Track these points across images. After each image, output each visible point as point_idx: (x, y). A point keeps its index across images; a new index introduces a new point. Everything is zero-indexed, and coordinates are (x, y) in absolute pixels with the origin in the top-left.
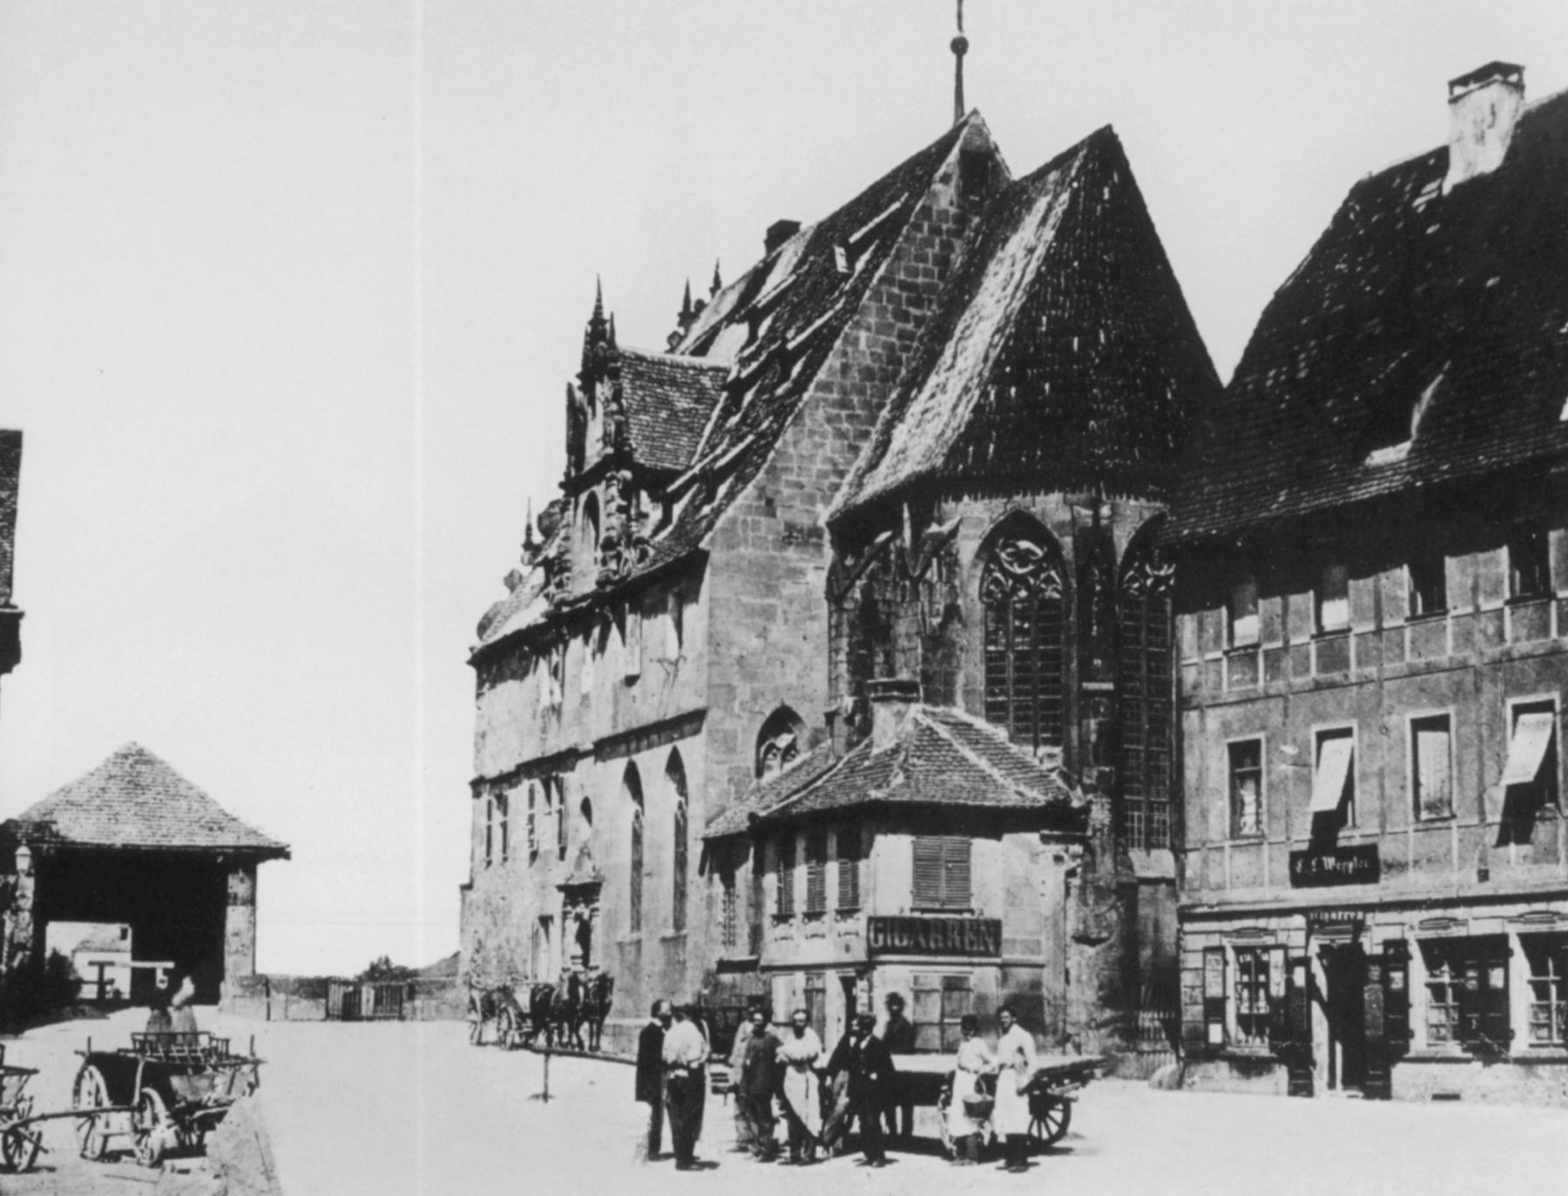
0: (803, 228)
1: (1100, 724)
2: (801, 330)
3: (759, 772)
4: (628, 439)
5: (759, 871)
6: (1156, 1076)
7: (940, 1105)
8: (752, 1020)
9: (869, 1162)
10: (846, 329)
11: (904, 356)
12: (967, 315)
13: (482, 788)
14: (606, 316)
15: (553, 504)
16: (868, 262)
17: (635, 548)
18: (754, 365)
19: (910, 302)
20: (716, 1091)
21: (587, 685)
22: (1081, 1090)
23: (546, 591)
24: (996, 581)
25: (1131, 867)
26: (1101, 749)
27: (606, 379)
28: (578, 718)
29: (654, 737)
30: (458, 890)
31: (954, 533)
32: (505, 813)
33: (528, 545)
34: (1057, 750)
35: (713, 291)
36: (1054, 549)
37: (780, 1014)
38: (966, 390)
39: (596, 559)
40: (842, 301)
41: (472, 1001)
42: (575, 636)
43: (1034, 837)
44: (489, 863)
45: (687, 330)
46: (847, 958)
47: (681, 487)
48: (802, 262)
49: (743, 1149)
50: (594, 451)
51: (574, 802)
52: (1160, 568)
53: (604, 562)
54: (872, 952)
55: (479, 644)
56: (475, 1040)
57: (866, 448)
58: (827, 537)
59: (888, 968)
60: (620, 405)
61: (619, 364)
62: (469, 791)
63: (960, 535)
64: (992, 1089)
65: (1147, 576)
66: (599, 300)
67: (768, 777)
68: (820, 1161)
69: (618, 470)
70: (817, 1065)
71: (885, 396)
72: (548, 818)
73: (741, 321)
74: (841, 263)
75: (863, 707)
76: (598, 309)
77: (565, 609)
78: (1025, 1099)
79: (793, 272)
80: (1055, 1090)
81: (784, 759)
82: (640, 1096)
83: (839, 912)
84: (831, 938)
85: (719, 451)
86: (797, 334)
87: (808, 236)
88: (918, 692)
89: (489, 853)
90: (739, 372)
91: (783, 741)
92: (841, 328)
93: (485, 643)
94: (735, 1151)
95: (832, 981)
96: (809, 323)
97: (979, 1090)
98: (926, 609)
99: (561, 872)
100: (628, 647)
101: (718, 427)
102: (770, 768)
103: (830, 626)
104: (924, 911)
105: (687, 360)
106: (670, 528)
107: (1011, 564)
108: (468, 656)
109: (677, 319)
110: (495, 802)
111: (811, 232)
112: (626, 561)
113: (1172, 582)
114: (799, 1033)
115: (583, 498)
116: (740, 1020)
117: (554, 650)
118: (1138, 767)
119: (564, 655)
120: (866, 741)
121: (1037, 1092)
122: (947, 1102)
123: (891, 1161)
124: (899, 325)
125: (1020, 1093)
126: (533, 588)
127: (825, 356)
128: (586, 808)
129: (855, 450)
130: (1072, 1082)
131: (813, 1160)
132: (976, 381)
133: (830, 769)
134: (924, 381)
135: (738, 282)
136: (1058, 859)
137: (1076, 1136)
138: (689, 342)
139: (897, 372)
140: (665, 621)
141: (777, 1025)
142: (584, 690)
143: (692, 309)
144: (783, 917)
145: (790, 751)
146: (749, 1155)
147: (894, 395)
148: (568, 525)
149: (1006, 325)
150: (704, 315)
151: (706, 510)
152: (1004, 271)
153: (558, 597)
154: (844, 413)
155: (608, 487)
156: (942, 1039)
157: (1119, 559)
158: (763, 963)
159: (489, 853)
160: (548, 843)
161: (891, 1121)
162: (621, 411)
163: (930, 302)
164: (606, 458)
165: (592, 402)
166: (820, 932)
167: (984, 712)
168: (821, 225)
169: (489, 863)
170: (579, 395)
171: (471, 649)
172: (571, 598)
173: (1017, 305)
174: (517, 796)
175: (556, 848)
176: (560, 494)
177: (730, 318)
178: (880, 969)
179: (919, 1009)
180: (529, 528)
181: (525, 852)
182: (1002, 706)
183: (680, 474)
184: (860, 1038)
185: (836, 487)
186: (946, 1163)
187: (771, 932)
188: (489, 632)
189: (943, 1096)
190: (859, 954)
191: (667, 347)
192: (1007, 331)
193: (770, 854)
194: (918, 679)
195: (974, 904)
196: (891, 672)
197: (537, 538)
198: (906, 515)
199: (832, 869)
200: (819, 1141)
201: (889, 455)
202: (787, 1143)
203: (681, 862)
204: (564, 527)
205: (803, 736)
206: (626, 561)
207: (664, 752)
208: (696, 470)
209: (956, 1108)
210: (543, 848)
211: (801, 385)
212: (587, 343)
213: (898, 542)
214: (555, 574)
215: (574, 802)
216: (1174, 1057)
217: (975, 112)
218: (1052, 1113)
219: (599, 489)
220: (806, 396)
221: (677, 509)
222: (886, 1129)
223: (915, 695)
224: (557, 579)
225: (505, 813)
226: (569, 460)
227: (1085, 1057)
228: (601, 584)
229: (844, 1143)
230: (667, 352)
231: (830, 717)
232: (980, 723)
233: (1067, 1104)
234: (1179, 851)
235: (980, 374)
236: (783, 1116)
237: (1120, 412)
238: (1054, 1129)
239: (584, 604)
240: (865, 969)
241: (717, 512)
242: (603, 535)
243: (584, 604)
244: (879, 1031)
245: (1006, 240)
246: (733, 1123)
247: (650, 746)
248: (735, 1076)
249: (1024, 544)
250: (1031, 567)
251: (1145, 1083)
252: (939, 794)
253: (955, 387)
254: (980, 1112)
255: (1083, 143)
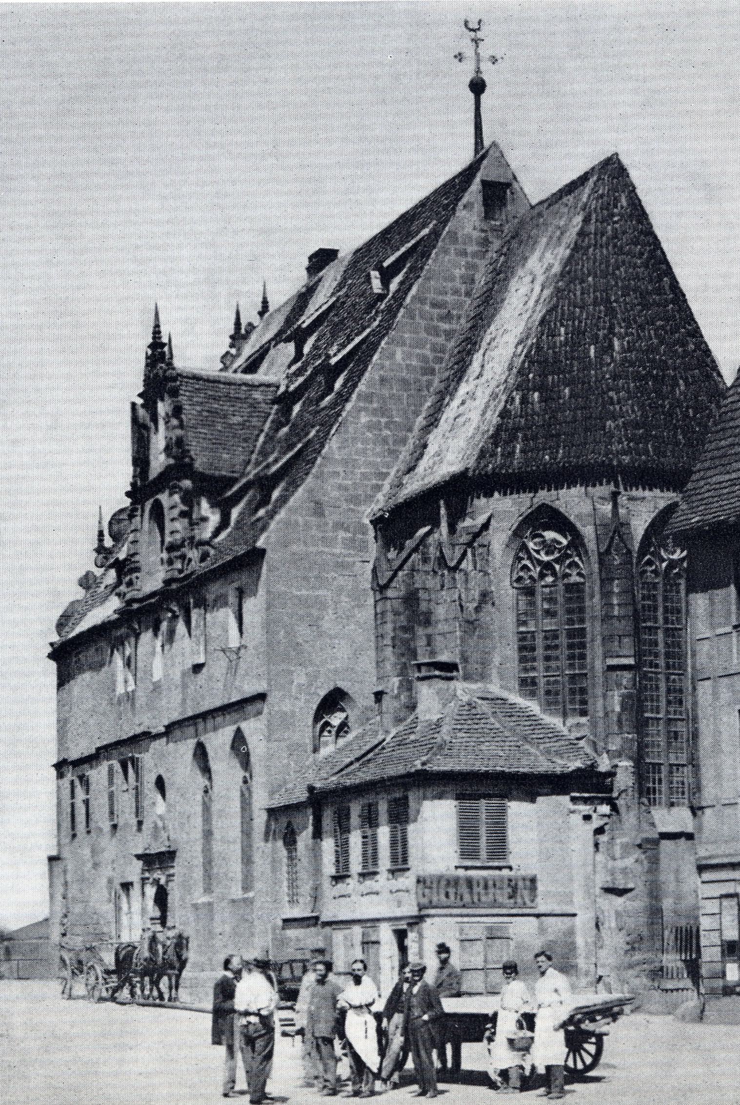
0: (340, 255)
1: (623, 696)
2: (343, 346)
3: (316, 750)
4: (189, 451)
5: (318, 834)
6: (679, 1011)
7: (485, 1041)
8: (315, 970)
9: (423, 1093)
10: (383, 343)
11: (437, 367)
12: (492, 328)
13: (64, 769)
14: (165, 340)
15: (122, 511)
16: (402, 283)
17: (197, 548)
18: (301, 380)
19: (442, 318)
20: (285, 1034)
21: (158, 674)
22: (612, 1024)
23: (117, 590)
24: (525, 567)
25: (653, 825)
26: (624, 717)
27: (166, 396)
28: (150, 706)
29: (219, 720)
30: (46, 862)
31: (486, 526)
32: (87, 792)
33: (100, 549)
34: (583, 720)
35: (261, 314)
36: (577, 542)
37: (340, 964)
38: (494, 396)
39: (162, 560)
40: (379, 319)
41: (63, 960)
42: (147, 629)
43: (565, 800)
44: (74, 836)
45: (239, 350)
46: (398, 913)
47: (237, 492)
48: (340, 287)
49: (310, 1085)
50: (159, 461)
51: (149, 779)
52: (673, 553)
53: (170, 562)
54: (421, 908)
55: (55, 638)
56: (66, 996)
57: (405, 453)
58: (371, 533)
59: (436, 920)
60: (181, 421)
61: (178, 383)
62: (53, 772)
63: (490, 531)
64: (531, 1027)
65: (663, 560)
66: (157, 326)
67: (324, 752)
68: (380, 1093)
69: (179, 480)
70: (375, 1008)
71: (421, 405)
72: (126, 794)
73: (288, 340)
74: (376, 285)
75: (407, 686)
76: (157, 332)
77: (136, 606)
78: (561, 1034)
79: (333, 294)
80: (587, 1026)
81: (337, 736)
82: (217, 1041)
83: (392, 872)
84: (385, 894)
85: (271, 459)
86: (339, 351)
87: (346, 263)
88: (458, 670)
89: (73, 827)
90: (288, 387)
91: (336, 719)
92: (379, 343)
93: (64, 639)
94: (302, 1087)
95: (386, 934)
96: (350, 340)
97: (521, 1027)
98: (463, 596)
99: (141, 843)
100: (194, 639)
101: (270, 438)
102: (326, 744)
103: (376, 614)
104: (467, 868)
105: (240, 376)
106: (229, 530)
107: (538, 552)
108: (49, 650)
109: (228, 341)
110: (77, 783)
111: (349, 257)
112: (190, 560)
113: (685, 565)
114: (358, 981)
115: (148, 505)
116: (305, 970)
117: (126, 643)
118: (658, 735)
119: (136, 648)
120: (412, 717)
121: (571, 1028)
122: (490, 1040)
123: (442, 1092)
124: (435, 340)
125: (556, 1030)
126: (106, 587)
127: (365, 369)
128: (160, 784)
129: (394, 454)
130: (604, 1017)
131: (373, 1093)
132: (502, 388)
133: (380, 743)
134: (456, 389)
135: (286, 303)
136: (587, 818)
137: (609, 1066)
138: (240, 362)
139: (429, 384)
140: (226, 616)
141: (339, 974)
142: (156, 678)
143: (243, 331)
144: (338, 878)
145: (343, 728)
146: (315, 1089)
147: (429, 404)
148: (135, 530)
149: (527, 338)
150: (254, 336)
151: (261, 512)
152: (523, 290)
153: (128, 597)
154: (383, 420)
155: (171, 495)
156: (485, 982)
157: (636, 546)
158: (324, 918)
159: (73, 827)
160: (127, 817)
161: (442, 1056)
162: (181, 426)
163: (459, 318)
164: (168, 468)
165: (155, 419)
166: (374, 890)
167: (517, 687)
168: (358, 251)
169: (74, 836)
170: (141, 412)
171: (52, 644)
172: (140, 595)
173: (538, 317)
174: (98, 775)
175: (134, 821)
176: (127, 502)
177: (278, 338)
178: (429, 921)
179: (466, 957)
180: (101, 534)
181: (106, 826)
182: (533, 681)
183: (235, 480)
184: (413, 983)
185: (378, 488)
186: (491, 1093)
187: (329, 890)
188: (67, 629)
189: (487, 1034)
190: (410, 909)
191: (221, 366)
192: (529, 342)
193: (328, 821)
194: (458, 661)
195: (512, 861)
196: (433, 653)
197: (108, 542)
198: (443, 511)
199: (384, 833)
200: (377, 1076)
201: (426, 458)
202: (348, 1079)
203: (247, 832)
204: (132, 531)
205: (352, 714)
206: (190, 560)
207: (226, 734)
208: (251, 476)
209: (500, 1043)
210: (121, 822)
211: (343, 398)
212: (147, 365)
213: (436, 536)
214: (126, 575)
215: (149, 779)
216: (695, 993)
217: (494, 144)
218: (586, 1046)
219: (164, 498)
220: (349, 406)
221: (235, 513)
222: (437, 1064)
223: (455, 674)
224: (127, 579)
225: (87, 792)
226: (135, 471)
227: (616, 996)
228: (167, 582)
229: (400, 1077)
230: (221, 370)
231: (379, 696)
232: (516, 698)
233: (600, 1037)
234: (696, 810)
235: (506, 381)
236: (345, 1055)
237: (633, 411)
238: (588, 1060)
239: (153, 600)
240: (417, 920)
241: (271, 515)
242: (168, 539)
243: (153, 600)
244: (430, 978)
245: (526, 259)
246: (300, 1062)
247: (215, 729)
248: (301, 1021)
249: (550, 535)
250: (557, 555)
251: (671, 1017)
252: (478, 763)
253: (482, 397)
254: (522, 1047)
255: (593, 169)
